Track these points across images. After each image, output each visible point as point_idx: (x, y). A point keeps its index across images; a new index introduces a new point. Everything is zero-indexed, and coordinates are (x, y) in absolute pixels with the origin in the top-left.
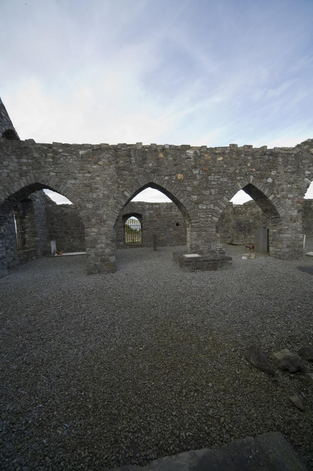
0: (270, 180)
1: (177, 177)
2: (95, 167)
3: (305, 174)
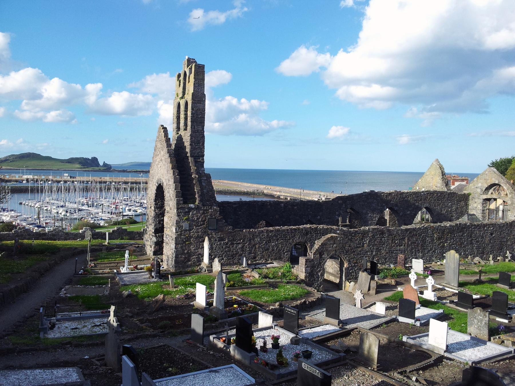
0: (319, 217)
1: (276, 217)
2: (240, 213)
3: (336, 214)
